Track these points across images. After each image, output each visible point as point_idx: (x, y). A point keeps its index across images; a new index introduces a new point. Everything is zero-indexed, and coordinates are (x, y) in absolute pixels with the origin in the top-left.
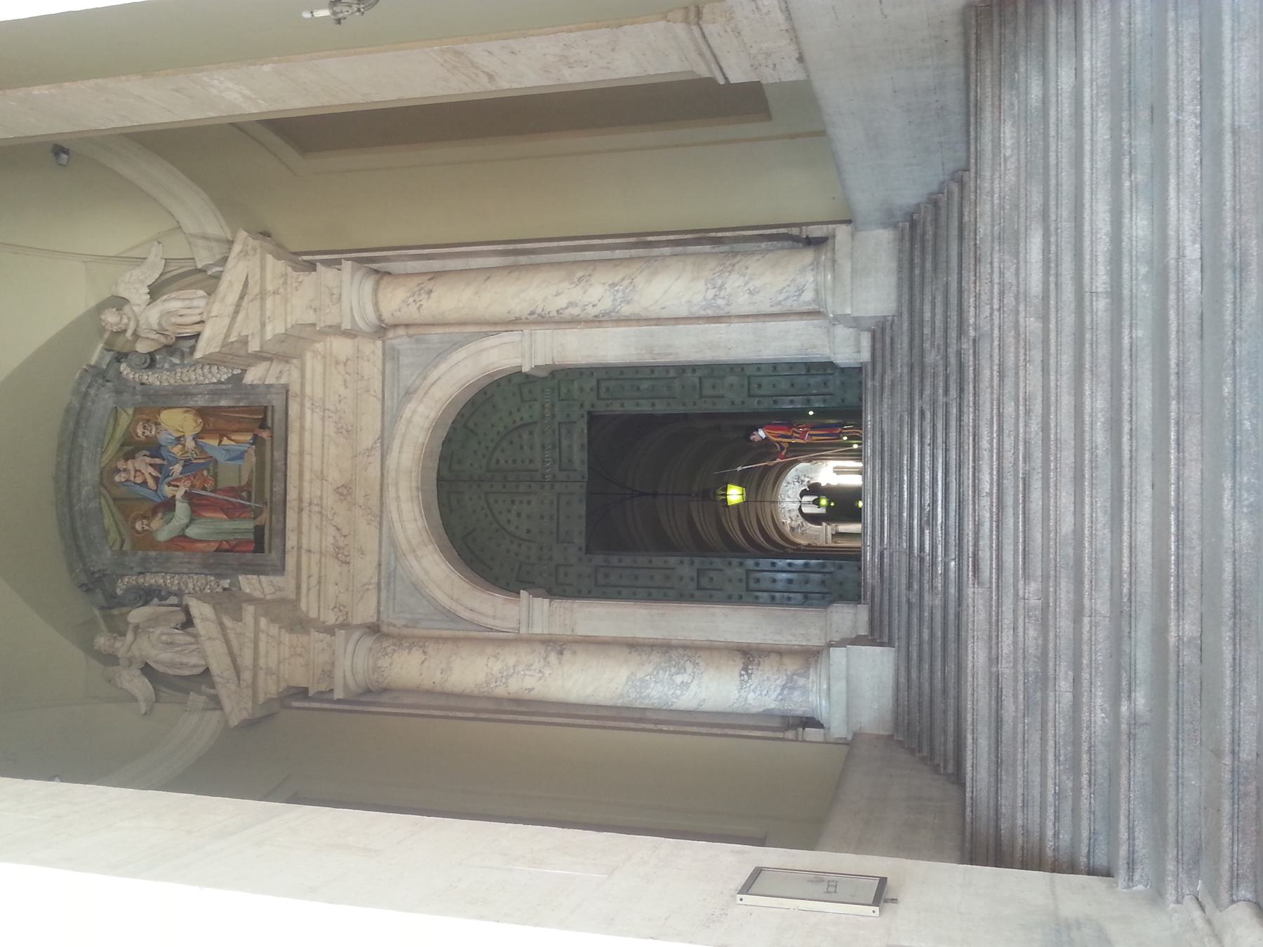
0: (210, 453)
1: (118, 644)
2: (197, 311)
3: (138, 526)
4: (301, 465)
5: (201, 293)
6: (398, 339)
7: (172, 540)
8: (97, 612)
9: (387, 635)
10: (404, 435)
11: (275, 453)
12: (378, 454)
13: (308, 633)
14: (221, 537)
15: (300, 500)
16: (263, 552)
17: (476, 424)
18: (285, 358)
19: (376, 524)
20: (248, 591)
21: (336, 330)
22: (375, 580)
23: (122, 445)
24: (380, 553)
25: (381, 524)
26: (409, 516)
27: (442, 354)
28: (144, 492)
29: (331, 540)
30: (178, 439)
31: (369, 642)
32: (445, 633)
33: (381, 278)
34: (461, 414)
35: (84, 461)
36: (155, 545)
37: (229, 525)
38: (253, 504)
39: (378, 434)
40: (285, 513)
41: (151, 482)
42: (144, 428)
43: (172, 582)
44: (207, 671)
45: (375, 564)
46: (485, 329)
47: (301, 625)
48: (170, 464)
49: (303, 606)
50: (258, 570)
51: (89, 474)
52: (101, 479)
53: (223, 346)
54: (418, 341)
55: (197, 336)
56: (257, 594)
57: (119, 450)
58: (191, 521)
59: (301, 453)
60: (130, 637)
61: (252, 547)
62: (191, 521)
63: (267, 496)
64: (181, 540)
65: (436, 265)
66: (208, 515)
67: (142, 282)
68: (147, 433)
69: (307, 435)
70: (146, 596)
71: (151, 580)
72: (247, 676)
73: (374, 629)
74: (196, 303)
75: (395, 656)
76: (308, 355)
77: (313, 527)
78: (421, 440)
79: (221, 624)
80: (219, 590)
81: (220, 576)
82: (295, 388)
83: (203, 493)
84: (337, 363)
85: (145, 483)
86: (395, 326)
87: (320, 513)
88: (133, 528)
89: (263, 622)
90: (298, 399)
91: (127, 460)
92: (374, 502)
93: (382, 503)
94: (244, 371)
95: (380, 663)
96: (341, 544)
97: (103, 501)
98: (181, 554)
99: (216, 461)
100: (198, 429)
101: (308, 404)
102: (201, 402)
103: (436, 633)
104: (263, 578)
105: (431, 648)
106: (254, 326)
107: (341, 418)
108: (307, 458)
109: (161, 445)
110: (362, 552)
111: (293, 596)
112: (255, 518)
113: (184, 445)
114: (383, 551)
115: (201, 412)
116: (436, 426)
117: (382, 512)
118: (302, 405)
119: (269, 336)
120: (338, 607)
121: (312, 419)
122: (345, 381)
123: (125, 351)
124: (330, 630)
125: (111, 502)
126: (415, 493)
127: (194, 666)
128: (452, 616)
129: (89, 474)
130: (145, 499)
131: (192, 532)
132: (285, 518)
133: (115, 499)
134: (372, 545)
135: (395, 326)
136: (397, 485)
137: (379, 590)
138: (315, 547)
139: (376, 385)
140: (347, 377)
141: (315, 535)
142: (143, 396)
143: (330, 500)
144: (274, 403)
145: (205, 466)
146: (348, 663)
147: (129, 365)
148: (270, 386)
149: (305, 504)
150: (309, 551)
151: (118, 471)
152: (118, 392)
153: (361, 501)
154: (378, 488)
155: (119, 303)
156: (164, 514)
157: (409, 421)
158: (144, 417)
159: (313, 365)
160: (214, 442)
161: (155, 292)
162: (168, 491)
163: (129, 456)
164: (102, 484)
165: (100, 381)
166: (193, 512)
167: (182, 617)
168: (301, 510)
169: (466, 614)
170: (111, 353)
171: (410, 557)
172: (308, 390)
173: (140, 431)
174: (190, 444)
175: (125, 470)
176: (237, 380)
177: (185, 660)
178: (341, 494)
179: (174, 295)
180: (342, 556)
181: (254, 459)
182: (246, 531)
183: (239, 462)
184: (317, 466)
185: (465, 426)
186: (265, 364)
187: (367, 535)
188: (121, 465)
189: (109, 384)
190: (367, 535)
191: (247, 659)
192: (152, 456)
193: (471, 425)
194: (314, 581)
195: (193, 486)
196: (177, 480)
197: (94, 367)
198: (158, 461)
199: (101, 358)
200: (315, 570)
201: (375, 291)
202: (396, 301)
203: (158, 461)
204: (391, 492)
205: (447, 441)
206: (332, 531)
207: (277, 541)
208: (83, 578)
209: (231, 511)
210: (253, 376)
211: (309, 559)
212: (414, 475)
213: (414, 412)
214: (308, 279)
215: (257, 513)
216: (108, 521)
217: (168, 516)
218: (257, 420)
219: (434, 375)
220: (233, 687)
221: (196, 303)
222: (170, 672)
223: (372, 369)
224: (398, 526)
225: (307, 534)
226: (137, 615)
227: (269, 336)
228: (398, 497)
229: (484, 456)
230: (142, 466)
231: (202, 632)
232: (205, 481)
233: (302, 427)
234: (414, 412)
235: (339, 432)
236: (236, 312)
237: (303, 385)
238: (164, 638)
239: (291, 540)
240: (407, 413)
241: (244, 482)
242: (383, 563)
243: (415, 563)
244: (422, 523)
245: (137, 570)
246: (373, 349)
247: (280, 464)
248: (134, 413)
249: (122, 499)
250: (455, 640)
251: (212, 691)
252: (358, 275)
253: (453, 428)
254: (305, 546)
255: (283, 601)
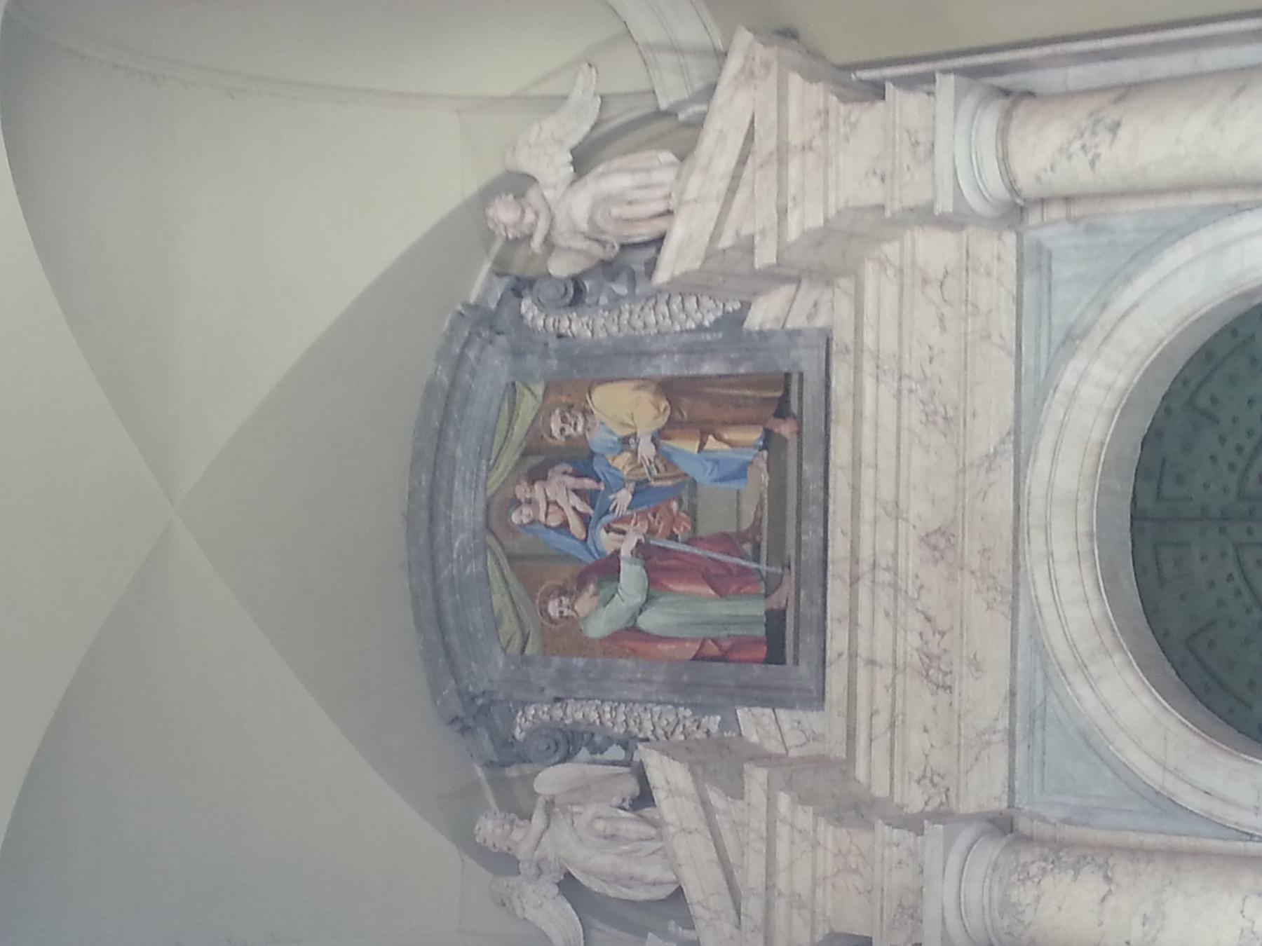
0: (684, 467)
1: (517, 835)
2: (660, 192)
3: (553, 609)
4: (855, 488)
5: (667, 156)
6: (1050, 229)
7: (613, 638)
8: (480, 772)
9: (1029, 839)
10: (1063, 425)
11: (805, 467)
12: (1008, 465)
13: (871, 827)
14: (710, 632)
15: (855, 559)
16: (782, 662)
17: (1213, 400)
18: (825, 277)
19: (1007, 610)
20: (754, 739)
21: (925, 216)
22: (1003, 723)
23: (525, 454)
24: (1013, 669)
25: (1014, 609)
26: (1074, 594)
27: (1144, 251)
28: (562, 542)
29: (914, 640)
30: (625, 441)
31: (992, 850)
32: (1150, 840)
33: (1015, 104)
34: (1181, 380)
35: (457, 484)
36: (583, 646)
37: (718, 609)
38: (763, 567)
39: (1009, 424)
40: (825, 586)
41: (575, 525)
42: (564, 420)
43: (615, 719)
44: (679, 892)
45: (1004, 691)
46: (1235, 197)
47: (856, 810)
48: (610, 489)
49: (861, 772)
50: (773, 698)
51: (466, 510)
52: (487, 517)
53: (707, 258)
54: (1090, 230)
55: (658, 241)
56: (773, 746)
57: (518, 465)
58: (649, 599)
59: (856, 464)
60: (538, 820)
61: (762, 651)
62: (649, 599)
63: (791, 552)
64: (630, 636)
65: (1129, 70)
66: (680, 588)
67: (560, 141)
68: (569, 430)
69: (867, 430)
70: (568, 742)
71: (575, 713)
72: (753, 907)
73: (1002, 825)
74: (657, 176)
75: (1047, 882)
76: (870, 269)
77: (880, 616)
78: (1096, 435)
79: (704, 803)
80: (700, 735)
81: (701, 709)
82: (844, 336)
83: (671, 545)
84: (925, 282)
85: (565, 525)
86: (1043, 201)
87: (895, 586)
88: (544, 612)
89: (784, 800)
90: (850, 357)
91: (532, 482)
92: (1002, 562)
93: (1016, 567)
94: (746, 306)
95: (1014, 895)
96: (936, 651)
97: (491, 562)
98: (629, 663)
99: (694, 483)
100: (662, 421)
101: (868, 366)
102: (666, 368)
103: (1133, 838)
104: (782, 714)
105: (1121, 869)
106: (766, 214)
107: (933, 393)
108: (867, 475)
109: (592, 454)
110: (976, 665)
111: (840, 752)
112: (767, 596)
113: (635, 453)
114: (1020, 666)
115: (668, 388)
116: (1129, 406)
117: (1016, 584)
118: (857, 369)
119: (793, 234)
120: (929, 777)
121: (877, 397)
122: (941, 319)
123: (530, 274)
124: (914, 824)
125: (504, 562)
126: (1084, 546)
127: (654, 884)
128: (1163, 805)
129: (466, 510)
130: (565, 557)
131: (651, 621)
132: (825, 596)
133: (511, 558)
134: (997, 653)
135: (1043, 201)
136: (1046, 529)
137: (1012, 746)
138: (883, 655)
139: (1005, 323)
140: (947, 311)
141: (883, 627)
142: (560, 360)
143: (912, 560)
144: (804, 366)
145: (675, 493)
146: (949, 891)
147: (537, 302)
148: (794, 334)
149: (864, 567)
150: (872, 662)
151: (517, 503)
152: (517, 353)
153: (974, 561)
154: (1008, 534)
155: (518, 184)
156: (599, 586)
157: (1073, 395)
158: (564, 399)
159: (879, 287)
160: (691, 447)
161: (583, 160)
162: (606, 541)
163: (537, 475)
164: (488, 527)
165: (485, 334)
166: (652, 582)
167: (631, 787)
168: (854, 580)
169: (1194, 802)
170: (506, 281)
171: (1076, 679)
172: (869, 338)
173: (555, 427)
174: (646, 450)
175: (530, 502)
176: (733, 322)
177: (637, 870)
178: (935, 548)
179: (617, 163)
180: (936, 672)
181: (765, 478)
182: (749, 622)
183: (735, 485)
184: (887, 493)
185: (1191, 403)
186: (786, 291)
187: (987, 632)
188: (522, 491)
189: (502, 340)
190: (987, 632)
191: (753, 874)
192: (577, 475)
193: (1203, 401)
194: (881, 722)
195: (651, 532)
196: (622, 520)
197: (476, 307)
198: (588, 483)
199: (487, 290)
200: (882, 700)
201: (1003, 132)
202: (1046, 149)
203: (588, 483)
204: (1035, 545)
205: (1153, 438)
206: (916, 622)
207: (809, 640)
208: (456, 707)
209: (723, 581)
210: (764, 314)
211: (872, 681)
212: (1082, 507)
213: (1083, 376)
214: (869, 116)
215: (773, 583)
216: (499, 600)
217: (606, 591)
218: (769, 400)
219: (1126, 297)
220: (727, 928)
221: (657, 176)
222: (611, 892)
223: (995, 292)
224: (1049, 613)
225: (866, 628)
226: (551, 779)
227: (793, 234)
228: (1050, 554)
229: (1232, 467)
230: (559, 494)
231: (670, 817)
232: (674, 521)
233: (858, 413)
234: (1083, 376)
235: (929, 419)
236: (732, 191)
237: (858, 330)
238: (600, 825)
239: (837, 641)
240: (1068, 379)
241: (746, 525)
242: (1020, 692)
243: (1084, 691)
244: (1099, 608)
245: (551, 693)
246: (997, 250)
247: (814, 487)
248: (545, 395)
249: (523, 557)
250: (1173, 855)
251: (687, 934)
252: (969, 102)
253: (1166, 408)
254: (863, 652)
255: (820, 762)
